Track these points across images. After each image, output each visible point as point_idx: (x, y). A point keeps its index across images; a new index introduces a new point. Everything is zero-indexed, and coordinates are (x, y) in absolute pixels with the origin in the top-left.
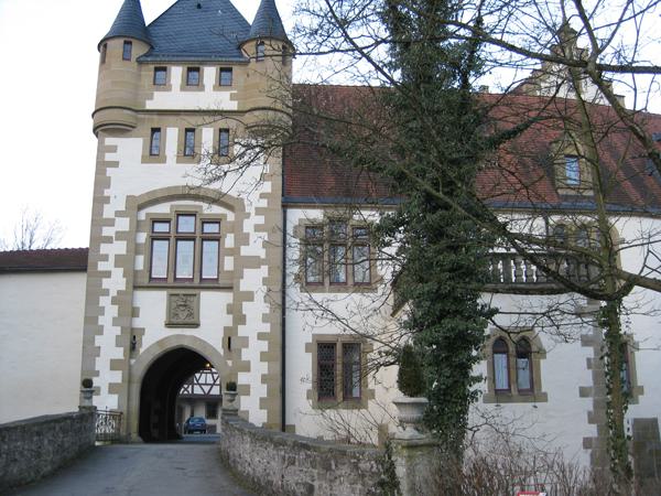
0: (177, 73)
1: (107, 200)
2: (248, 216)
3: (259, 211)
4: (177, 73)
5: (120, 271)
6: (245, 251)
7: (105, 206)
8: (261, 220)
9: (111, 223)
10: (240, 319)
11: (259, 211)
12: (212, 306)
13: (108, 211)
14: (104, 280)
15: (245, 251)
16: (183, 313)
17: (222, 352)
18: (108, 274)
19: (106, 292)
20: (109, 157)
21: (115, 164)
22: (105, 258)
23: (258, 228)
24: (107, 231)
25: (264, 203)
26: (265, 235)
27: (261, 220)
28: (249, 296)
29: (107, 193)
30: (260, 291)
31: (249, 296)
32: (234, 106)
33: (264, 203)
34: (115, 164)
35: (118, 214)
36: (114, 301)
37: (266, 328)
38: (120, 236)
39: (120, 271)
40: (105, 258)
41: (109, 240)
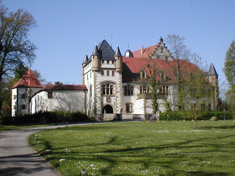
0: (105, 62)
1: (96, 82)
2: (117, 85)
3: (119, 84)
4: (105, 62)
5: (99, 93)
6: (117, 90)
7: (96, 83)
8: (119, 85)
9: (97, 86)
10: (117, 100)
11: (119, 84)
12: (113, 99)
13: (97, 84)
14: (97, 95)
15: (117, 90)
16: (108, 99)
17: (114, 105)
18: (97, 94)
19: (97, 96)
20: (96, 75)
21: (97, 76)
22: (97, 91)
23: (119, 87)
24: (97, 87)
25: (119, 83)
26: (120, 88)
27: (119, 85)
28: (118, 97)
29: (96, 81)
30: (119, 96)
31: (118, 97)
32: (114, 67)
33: (119, 83)
34: (97, 76)
35: (98, 84)
36: (99, 98)
37: (120, 102)
38: (99, 88)
39: (99, 93)
40: (97, 91)
41: (97, 88)
